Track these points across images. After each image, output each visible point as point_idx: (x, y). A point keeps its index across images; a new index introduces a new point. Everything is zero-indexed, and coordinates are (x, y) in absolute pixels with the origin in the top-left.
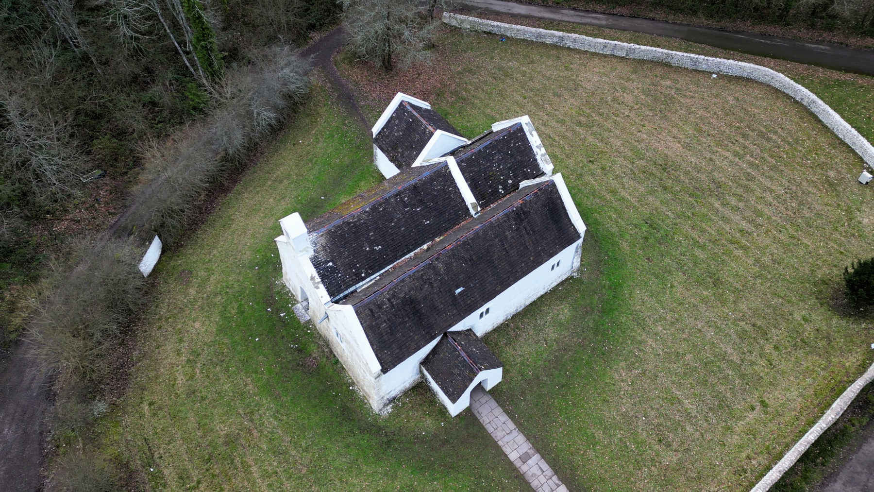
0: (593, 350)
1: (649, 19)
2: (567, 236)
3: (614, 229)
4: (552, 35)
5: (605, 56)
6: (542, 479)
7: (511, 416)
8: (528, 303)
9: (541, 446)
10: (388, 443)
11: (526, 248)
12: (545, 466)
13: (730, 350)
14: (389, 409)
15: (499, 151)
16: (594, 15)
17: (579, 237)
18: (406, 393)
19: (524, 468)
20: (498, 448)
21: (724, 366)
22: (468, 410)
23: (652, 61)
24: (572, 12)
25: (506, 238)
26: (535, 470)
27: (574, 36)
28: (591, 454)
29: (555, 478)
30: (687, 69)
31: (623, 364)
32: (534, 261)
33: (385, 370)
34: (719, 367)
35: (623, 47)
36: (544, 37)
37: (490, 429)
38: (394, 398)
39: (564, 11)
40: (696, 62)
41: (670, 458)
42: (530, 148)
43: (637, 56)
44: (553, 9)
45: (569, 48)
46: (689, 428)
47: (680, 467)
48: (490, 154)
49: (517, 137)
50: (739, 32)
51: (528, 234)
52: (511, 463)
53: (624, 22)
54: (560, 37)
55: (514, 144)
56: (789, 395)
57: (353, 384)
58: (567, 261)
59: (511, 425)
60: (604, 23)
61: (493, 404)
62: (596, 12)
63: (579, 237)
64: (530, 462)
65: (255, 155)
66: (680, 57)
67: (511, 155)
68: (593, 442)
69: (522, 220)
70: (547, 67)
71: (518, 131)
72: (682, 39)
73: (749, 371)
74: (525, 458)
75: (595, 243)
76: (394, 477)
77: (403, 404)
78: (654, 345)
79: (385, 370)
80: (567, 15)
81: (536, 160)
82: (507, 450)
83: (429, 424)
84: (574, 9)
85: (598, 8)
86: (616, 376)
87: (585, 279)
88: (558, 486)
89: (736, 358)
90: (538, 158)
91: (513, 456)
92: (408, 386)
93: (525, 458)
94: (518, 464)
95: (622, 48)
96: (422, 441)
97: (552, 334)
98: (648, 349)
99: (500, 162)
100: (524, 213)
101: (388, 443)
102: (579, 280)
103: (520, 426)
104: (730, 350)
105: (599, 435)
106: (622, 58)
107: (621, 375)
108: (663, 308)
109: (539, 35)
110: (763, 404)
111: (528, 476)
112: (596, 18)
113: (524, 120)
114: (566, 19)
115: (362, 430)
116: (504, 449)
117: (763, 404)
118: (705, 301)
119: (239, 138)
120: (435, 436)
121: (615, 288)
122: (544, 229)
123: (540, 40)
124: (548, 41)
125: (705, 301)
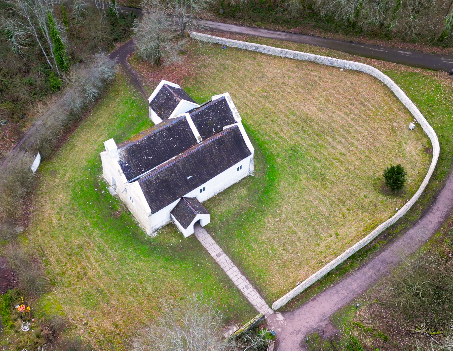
0: (256, 210)
1: (310, 35)
2: (249, 153)
4: (252, 46)
5: (282, 58)
6: (226, 264)
7: (214, 238)
8: (226, 188)
9: (227, 251)
10: (155, 248)
11: (223, 158)
12: (228, 258)
13: (324, 210)
14: (155, 234)
15: (213, 111)
16: (279, 33)
17: (251, 154)
18: (163, 227)
19: (217, 260)
20: (206, 251)
21: (320, 217)
22: (193, 235)
23: (308, 61)
24: (266, 31)
25: (213, 153)
26: (223, 260)
27: (264, 46)
28: (250, 254)
30: (327, 65)
31: (270, 216)
32: (227, 165)
33: (153, 212)
34: (318, 218)
35: (291, 53)
36: (247, 46)
37: (203, 243)
38: (158, 229)
39: (262, 30)
40: (331, 62)
41: (287, 257)
42: (230, 109)
43: (299, 58)
44: (255, 29)
45: (261, 53)
46: (299, 244)
47: (292, 260)
48: (208, 112)
49: (223, 104)
50: (360, 44)
51: (224, 151)
52: (212, 257)
53: (295, 37)
54: (256, 47)
55: (221, 107)
56: (350, 230)
57: (138, 223)
58: (245, 167)
59: (213, 241)
60: (284, 37)
61: (205, 232)
62: (280, 31)
63: (251, 154)
64: (221, 257)
65: (86, 112)
66: (323, 59)
67: (219, 113)
68: (251, 249)
69: (221, 144)
70: (248, 64)
71: (223, 102)
72: (327, 47)
73: (332, 219)
74: (219, 255)
75: (262, 158)
76: (157, 262)
77: (162, 232)
78: (287, 208)
79: (153, 212)
80: (263, 33)
81: (232, 115)
82: (210, 252)
83: (174, 241)
84: (268, 29)
85: (281, 28)
86: (266, 221)
87: (256, 176)
88: (233, 267)
89: (327, 214)
90: (234, 114)
91: (213, 255)
92: (164, 224)
93: (219, 255)
94: (215, 258)
95: (290, 54)
96: (171, 248)
97: (237, 202)
98: (284, 210)
99: (214, 116)
100: (222, 141)
101: (155, 248)
102: (253, 177)
103: (217, 242)
104: (324, 210)
105: (255, 246)
106: (291, 59)
107: (268, 221)
108: (294, 191)
109: (245, 46)
110: (337, 234)
111: (220, 263)
112: (279, 34)
113: (226, 95)
114: (262, 35)
115: (142, 243)
116: (209, 251)
117: (337, 234)
118: (316, 187)
119: (78, 103)
120: (177, 246)
121: (271, 181)
122: (233, 150)
123: (245, 48)
124: (250, 49)
125: (316, 187)
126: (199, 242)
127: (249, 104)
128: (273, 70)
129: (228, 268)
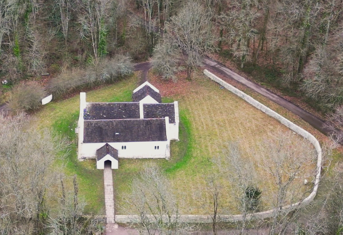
5: (257, 109)
6: (109, 191)
7: (113, 177)
9: (115, 186)
14: (82, 160)
18: (89, 159)
19: (106, 187)
22: (103, 170)
23: (274, 118)
29: (112, 193)
37: (105, 176)
38: (85, 158)
43: (269, 114)
45: (246, 101)
52: (104, 185)
61: (111, 172)
64: (109, 187)
70: (229, 103)
77: (87, 161)
82: (105, 182)
92: (91, 157)
95: (264, 108)
102: (167, 161)
103: (113, 179)
106: (264, 113)
120: (90, 171)
121: (177, 167)
126: (103, 175)
127: (204, 124)
128: (241, 113)
129: (108, 193)
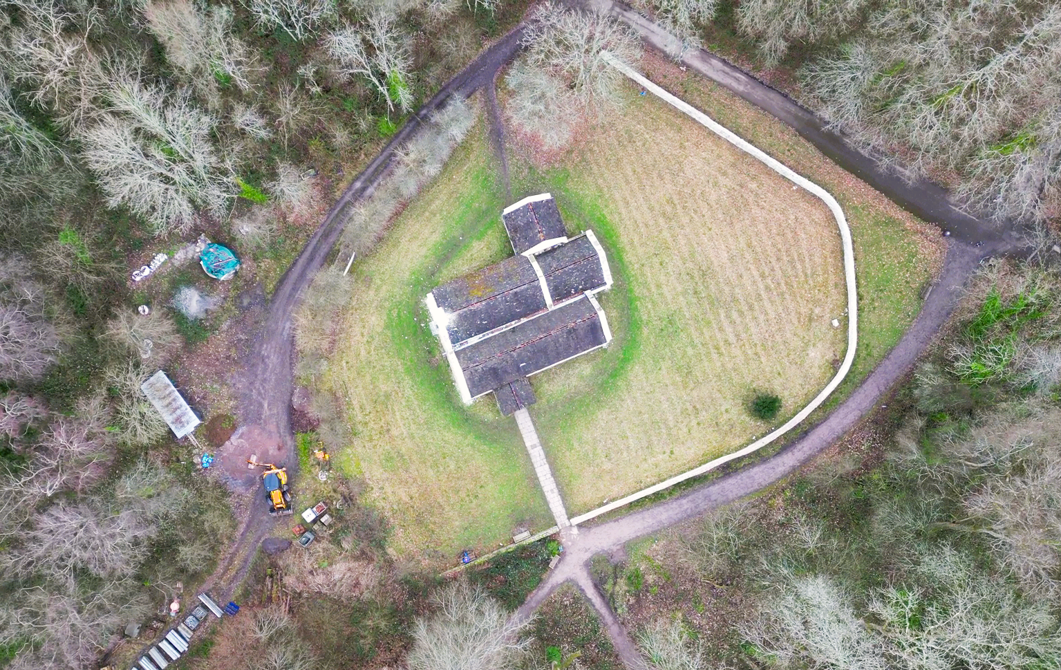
3: (645, 318)
